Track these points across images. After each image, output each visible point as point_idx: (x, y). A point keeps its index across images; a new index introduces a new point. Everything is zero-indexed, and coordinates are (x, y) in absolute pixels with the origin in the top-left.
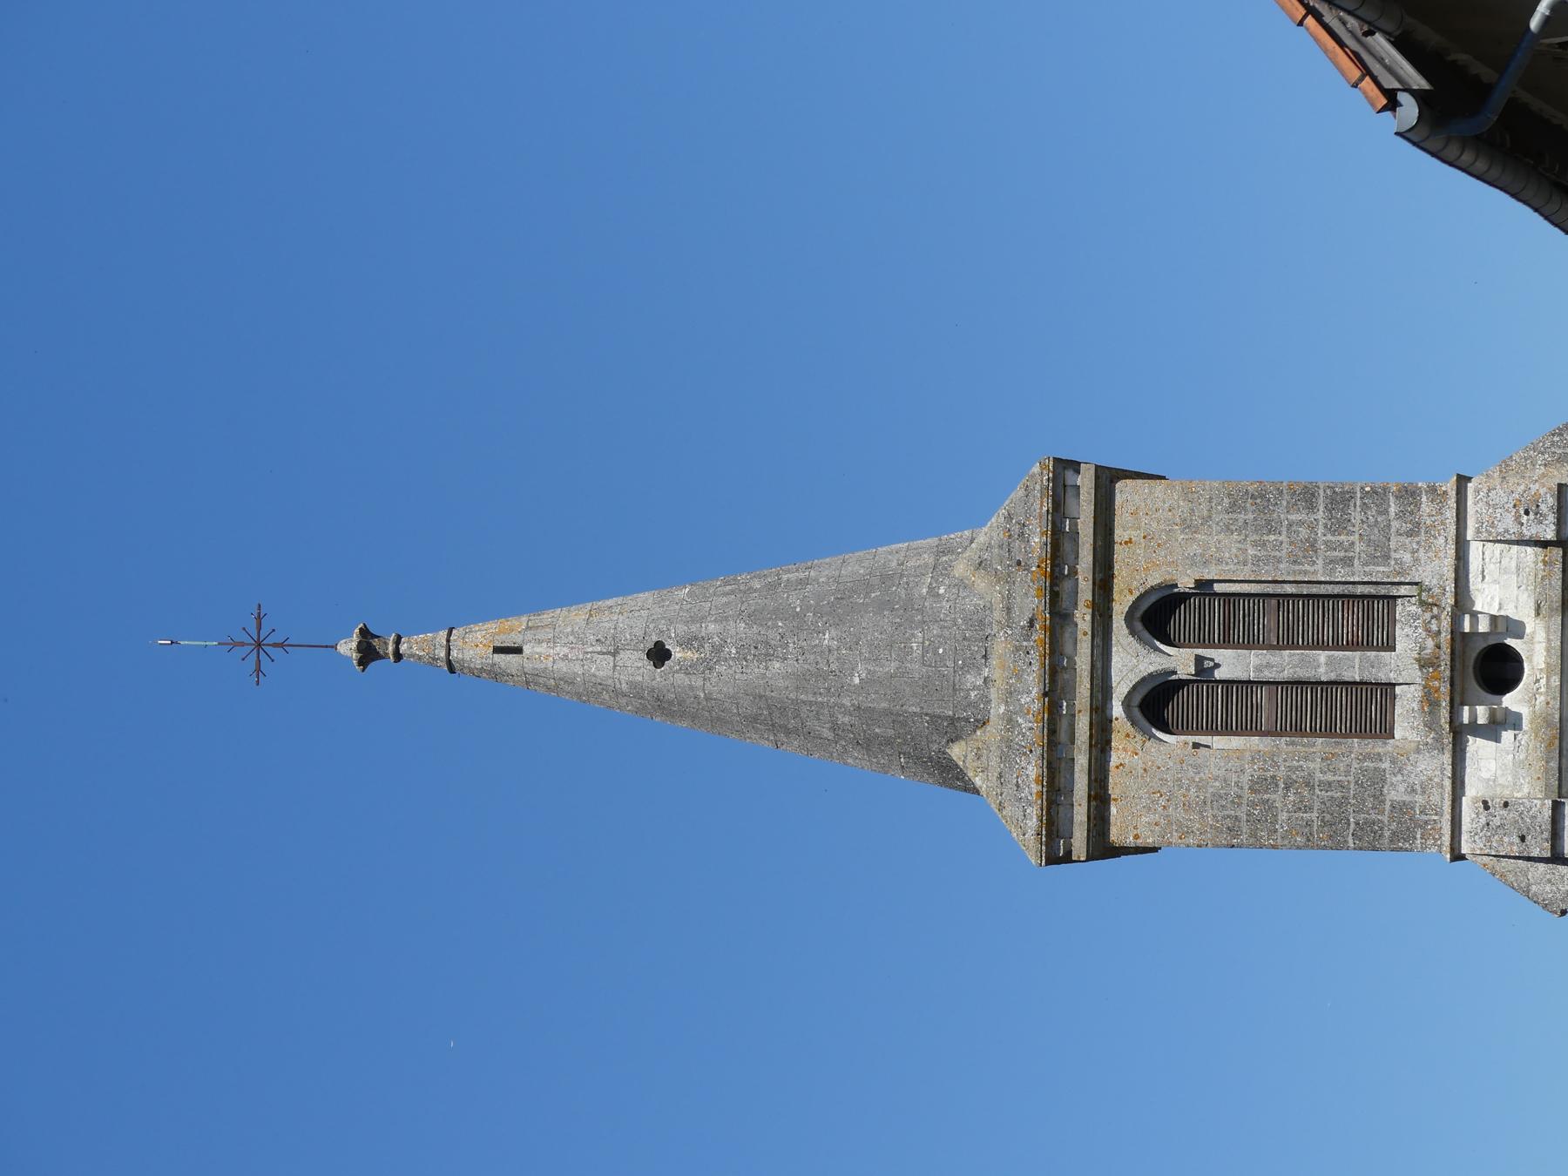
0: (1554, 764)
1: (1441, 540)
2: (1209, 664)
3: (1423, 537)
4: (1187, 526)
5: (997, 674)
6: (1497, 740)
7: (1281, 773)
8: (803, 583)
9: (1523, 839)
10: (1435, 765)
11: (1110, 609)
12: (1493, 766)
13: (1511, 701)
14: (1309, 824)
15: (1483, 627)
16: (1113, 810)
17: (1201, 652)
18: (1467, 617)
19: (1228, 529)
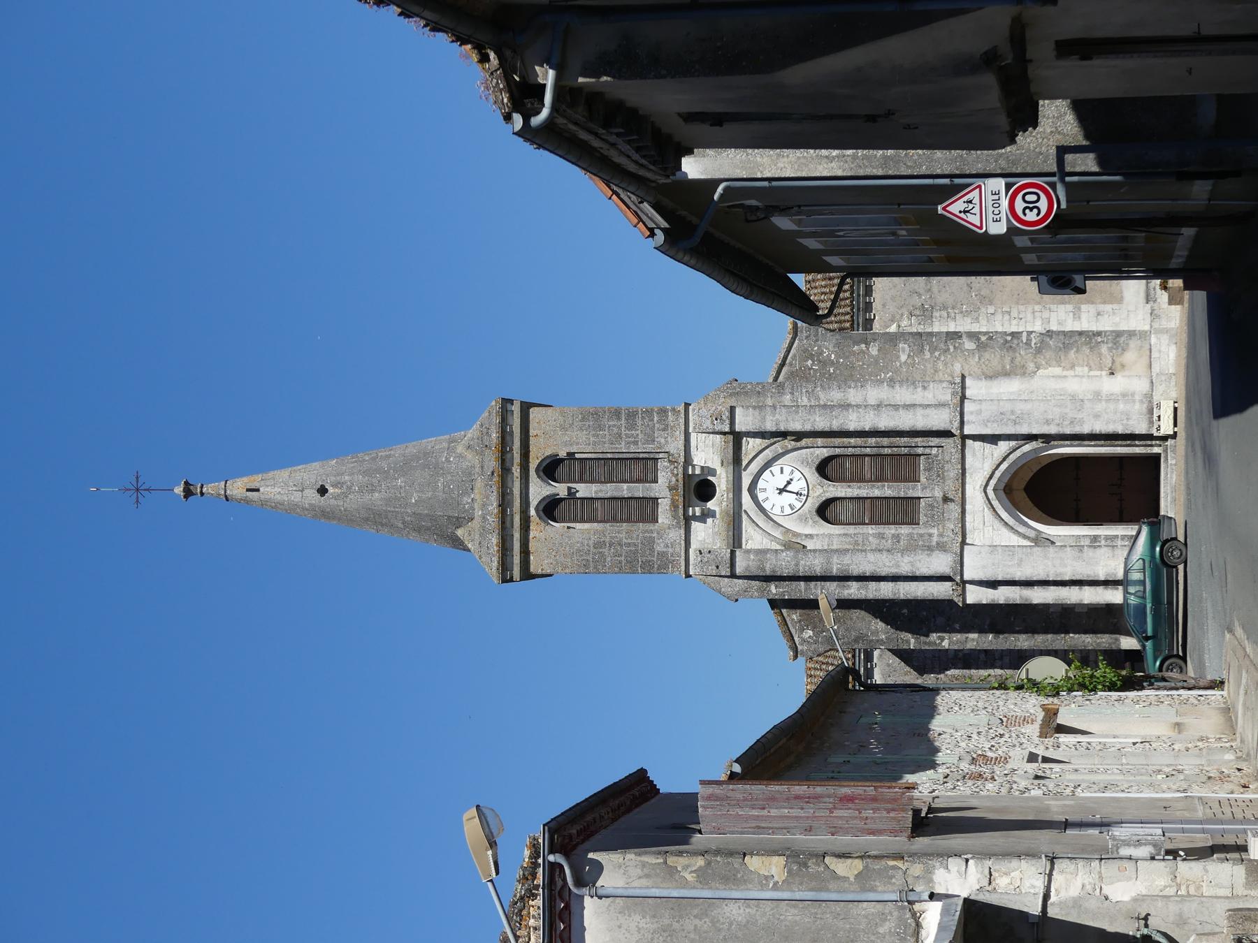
0: (731, 533)
1: (678, 432)
2: (573, 491)
3: (669, 431)
4: (563, 428)
5: (477, 497)
6: (705, 523)
7: (607, 540)
8: (388, 457)
9: (717, 567)
10: (677, 535)
11: (528, 466)
12: (703, 534)
13: (711, 505)
14: (620, 562)
15: (698, 472)
16: (532, 558)
17: (570, 485)
18: (690, 467)
19: (581, 429)
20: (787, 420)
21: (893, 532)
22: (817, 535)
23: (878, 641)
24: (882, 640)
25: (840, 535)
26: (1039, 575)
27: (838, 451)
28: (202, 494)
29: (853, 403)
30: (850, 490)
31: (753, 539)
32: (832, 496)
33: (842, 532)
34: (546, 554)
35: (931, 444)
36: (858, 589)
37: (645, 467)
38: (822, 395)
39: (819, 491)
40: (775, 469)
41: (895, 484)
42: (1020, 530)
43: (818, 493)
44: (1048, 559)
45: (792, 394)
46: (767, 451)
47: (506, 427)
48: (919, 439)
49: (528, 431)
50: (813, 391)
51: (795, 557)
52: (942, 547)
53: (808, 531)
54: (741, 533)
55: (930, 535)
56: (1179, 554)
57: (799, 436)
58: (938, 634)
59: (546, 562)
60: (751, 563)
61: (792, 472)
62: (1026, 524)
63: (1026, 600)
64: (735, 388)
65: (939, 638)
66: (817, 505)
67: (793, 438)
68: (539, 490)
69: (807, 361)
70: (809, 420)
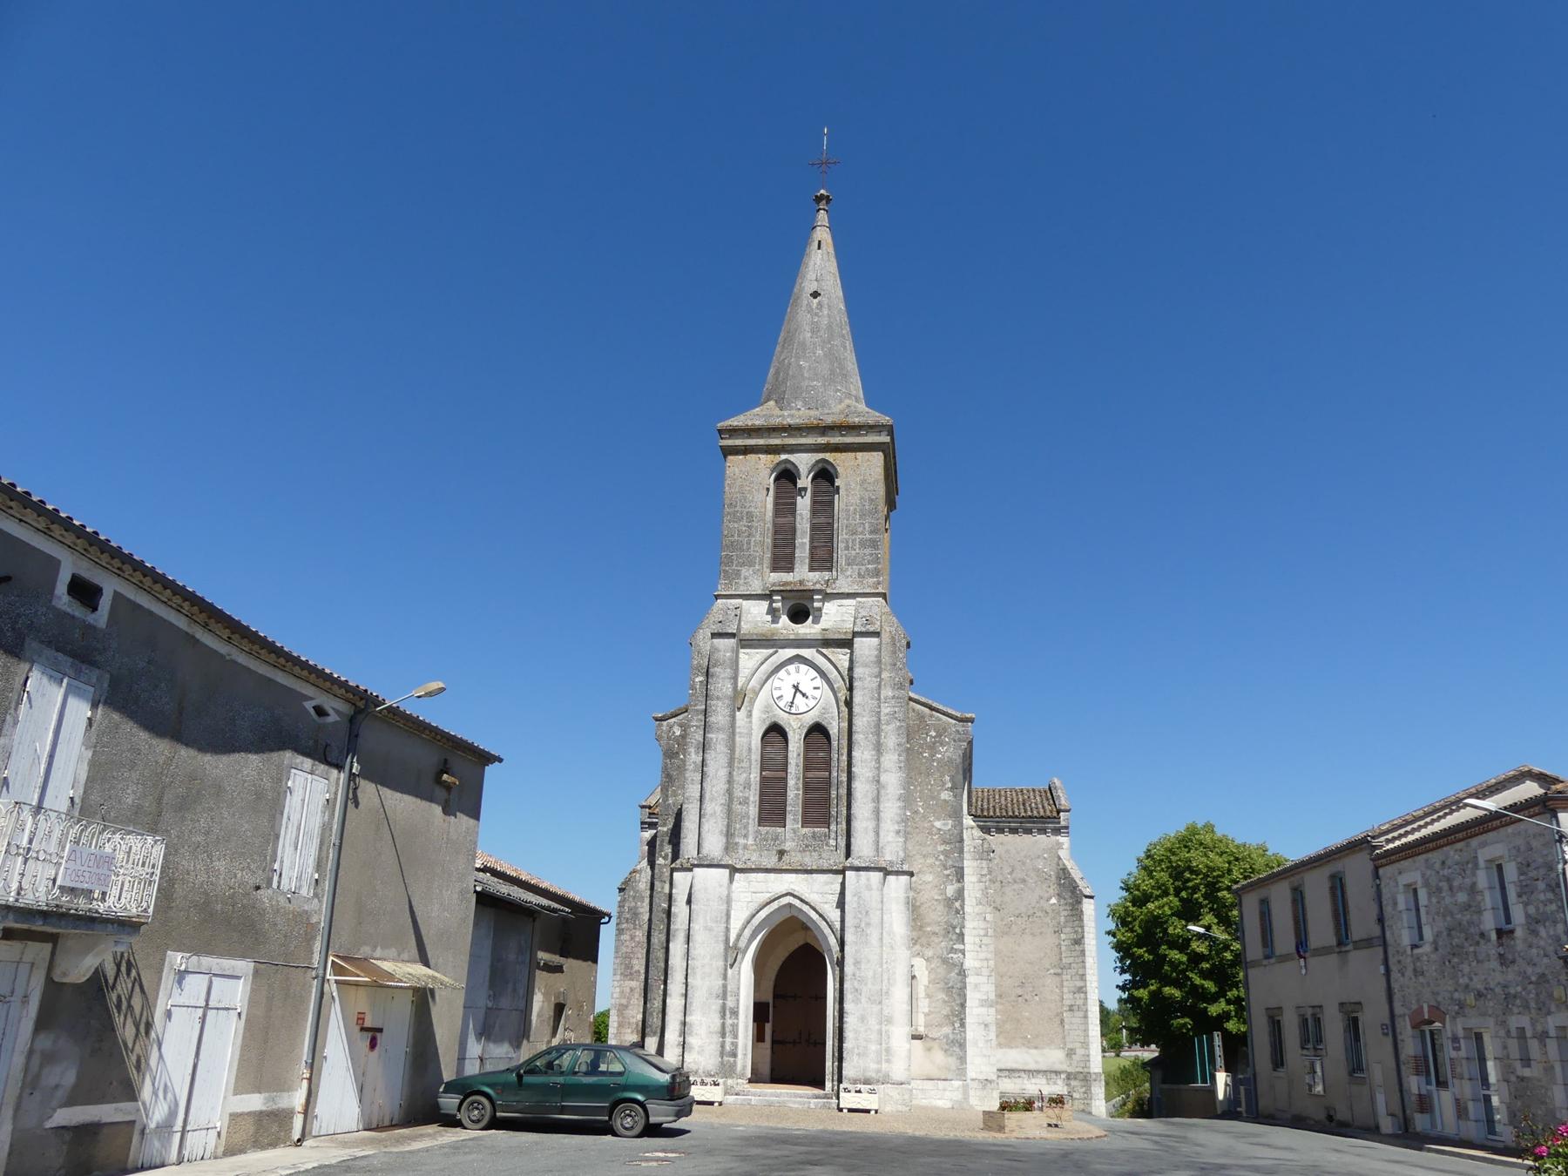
0: (755, 637)
1: (856, 587)
2: (803, 493)
3: (858, 579)
4: (864, 481)
5: (801, 412)
6: (767, 614)
7: (755, 524)
8: (845, 347)
9: (720, 622)
10: (756, 587)
11: (827, 452)
12: (756, 612)
13: (784, 619)
14: (732, 536)
15: (816, 605)
16: (741, 457)
17: (809, 490)
18: (820, 597)
19: (861, 498)
20: (865, 689)
21: (751, 799)
22: (751, 722)
23: (667, 796)
24: (667, 800)
25: (750, 744)
26: (695, 949)
27: (834, 744)
28: (818, 211)
29: (882, 759)
30: (795, 756)
31: (749, 659)
32: (789, 738)
33: (753, 747)
34: (743, 469)
35: (839, 838)
36: (694, 763)
37: (823, 558)
38: (891, 727)
39: (795, 725)
40: (819, 682)
41: (801, 801)
42: (746, 930)
43: (793, 723)
44: (711, 959)
45: (893, 697)
46: (836, 673)
47: (864, 430)
48: (844, 826)
49: (861, 451)
50: (896, 718)
51: (726, 697)
52: (729, 847)
53: (756, 713)
54: (755, 648)
55: (745, 836)
56: (627, 1126)
57: (849, 703)
58: (670, 854)
59: (736, 469)
60: (722, 653)
61: (814, 698)
62: (753, 937)
63: (674, 936)
64: (900, 641)
65: (667, 855)
66: (781, 723)
67: (848, 698)
68: (804, 462)
69: (935, 731)
70: (864, 711)
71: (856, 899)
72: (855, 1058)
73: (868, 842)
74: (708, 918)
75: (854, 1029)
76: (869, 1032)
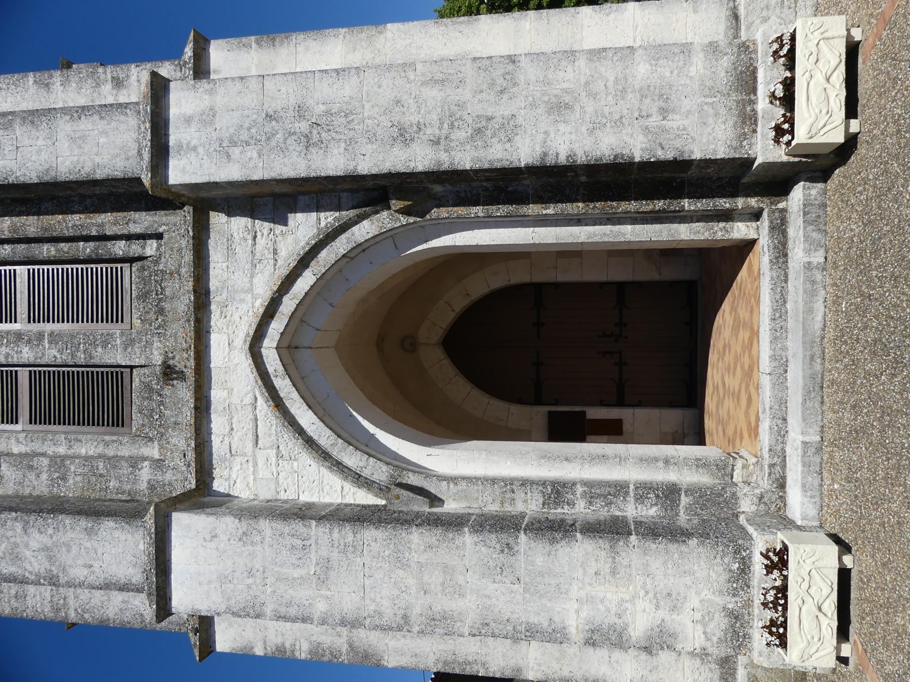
44: (405, 566)
71: (236, 152)
72: (675, 122)
73: (104, 133)
74: (297, 573)
75: (591, 132)
76: (599, 86)
